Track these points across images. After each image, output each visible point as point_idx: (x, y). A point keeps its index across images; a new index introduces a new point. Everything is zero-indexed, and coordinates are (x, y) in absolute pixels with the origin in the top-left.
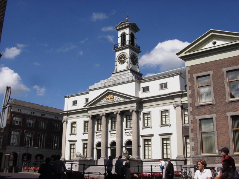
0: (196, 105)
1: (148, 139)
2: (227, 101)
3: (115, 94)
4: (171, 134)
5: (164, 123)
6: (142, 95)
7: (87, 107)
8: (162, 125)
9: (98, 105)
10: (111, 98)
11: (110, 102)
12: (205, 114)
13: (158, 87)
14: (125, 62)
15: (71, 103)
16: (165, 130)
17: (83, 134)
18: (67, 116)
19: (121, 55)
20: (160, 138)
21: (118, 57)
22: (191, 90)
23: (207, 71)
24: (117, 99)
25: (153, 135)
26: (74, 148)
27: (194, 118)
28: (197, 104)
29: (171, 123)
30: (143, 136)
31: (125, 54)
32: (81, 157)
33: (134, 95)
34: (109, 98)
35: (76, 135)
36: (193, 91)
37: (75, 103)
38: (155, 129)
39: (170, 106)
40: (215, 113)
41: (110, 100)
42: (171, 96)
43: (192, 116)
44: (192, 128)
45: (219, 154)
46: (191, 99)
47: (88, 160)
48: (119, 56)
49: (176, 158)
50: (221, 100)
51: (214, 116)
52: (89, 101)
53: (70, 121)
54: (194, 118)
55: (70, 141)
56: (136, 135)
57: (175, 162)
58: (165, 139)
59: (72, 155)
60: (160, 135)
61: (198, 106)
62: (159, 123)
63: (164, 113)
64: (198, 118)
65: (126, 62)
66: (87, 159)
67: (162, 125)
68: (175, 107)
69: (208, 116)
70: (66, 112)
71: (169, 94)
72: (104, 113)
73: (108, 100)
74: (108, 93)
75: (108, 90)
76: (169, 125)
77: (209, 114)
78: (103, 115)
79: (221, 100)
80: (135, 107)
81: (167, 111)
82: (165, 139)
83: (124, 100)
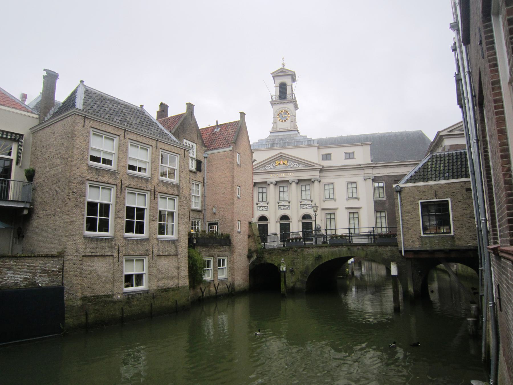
1: (331, 214)
4: (360, 208)
6: (326, 164)
8: (348, 199)
9: (262, 170)
10: (284, 164)
11: (282, 167)
16: (353, 204)
20: (346, 213)
24: (292, 166)
29: (359, 196)
33: (317, 162)
34: (282, 164)
39: (358, 177)
41: (282, 165)
42: (361, 167)
58: (354, 213)
62: (346, 197)
68: (365, 180)
71: (360, 165)
72: (274, 180)
75: (281, 153)
76: (357, 198)
78: (272, 183)
82: (354, 213)
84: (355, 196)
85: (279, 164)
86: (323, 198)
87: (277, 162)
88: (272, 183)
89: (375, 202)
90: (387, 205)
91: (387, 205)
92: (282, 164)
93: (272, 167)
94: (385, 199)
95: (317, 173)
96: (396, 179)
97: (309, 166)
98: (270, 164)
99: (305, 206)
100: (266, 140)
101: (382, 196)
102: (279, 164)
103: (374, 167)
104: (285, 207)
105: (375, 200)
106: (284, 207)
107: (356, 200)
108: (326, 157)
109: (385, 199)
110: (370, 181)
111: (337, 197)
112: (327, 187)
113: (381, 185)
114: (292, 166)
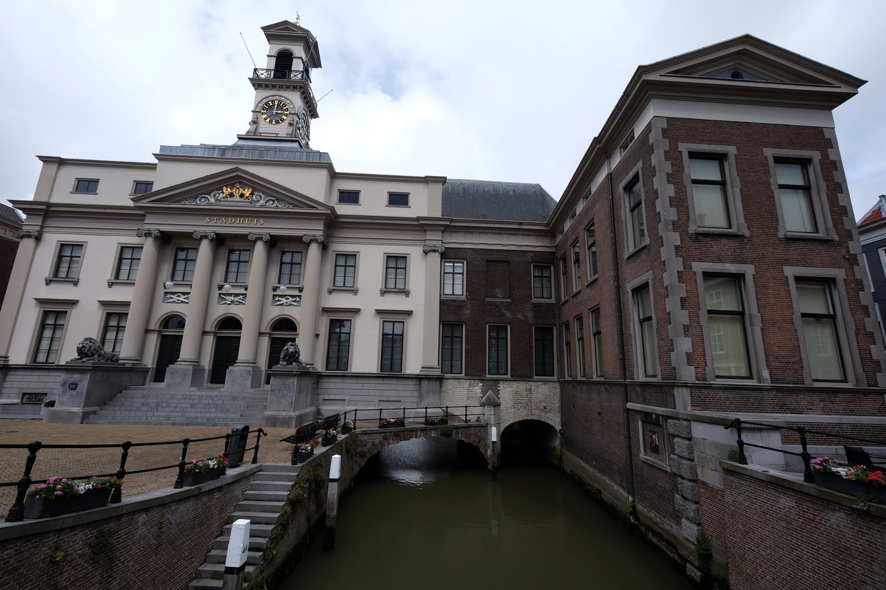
0: (692, 229)
3: (260, 186)
4: (409, 313)
5: (391, 285)
7: (144, 203)
9: (188, 204)
10: (242, 196)
11: (236, 203)
12: (720, 260)
13: (385, 199)
14: (282, 120)
15: (71, 184)
17: (111, 285)
18: (44, 221)
19: (273, 101)
21: (263, 103)
23: (721, 143)
24: (262, 202)
25: (360, 310)
26: (56, 327)
27: (687, 266)
30: (326, 311)
32: (99, 355)
33: (322, 200)
34: (237, 195)
35: (76, 283)
37: (87, 186)
38: (368, 296)
40: (752, 263)
42: (419, 226)
43: (681, 259)
44: (684, 295)
47: (127, 366)
49: (417, 372)
52: (155, 188)
53: (52, 241)
54: (687, 266)
55: (40, 301)
57: (415, 382)
59: (45, 345)
60: (379, 312)
62: (379, 284)
63: (396, 264)
64: (698, 267)
65: (286, 123)
66: (124, 364)
67: (383, 293)
68: (426, 253)
69: (731, 268)
70: (44, 207)
71: (418, 219)
73: (229, 199)
74: (235, 179)
75: (237, 169)
76: (407, 293)
77: (732, 262)
78: (205, 237)
80: (321, 233)
81: (404, 258)
83: (288, 208)
84: (400, 285)
85: (231, 195)
86: (328, 284)
87: (227, 190)
88: (205, 237)
89: (444, 303)
90: (467, 312)
91: (467, 312)
92: (237, 195)
93: (212, 200)
94: (464, 298)
95: (320, 226)
96: (490, 258)
97: (298, 206)
98: (209, 194)
99: (284, 300)
100: (224, 149)
101: (458, 291)
102: (231, 195)
103: (446, 226)
104: (236, 299)
105: (443, 297)
106: (232, 298)
107: (402, 297)
108: (350, 197)
109: (464, 298)
110: (436, 257)
111: (361, 284)
112: (341, 262)
113: (460, 267)
114: (262, 202)
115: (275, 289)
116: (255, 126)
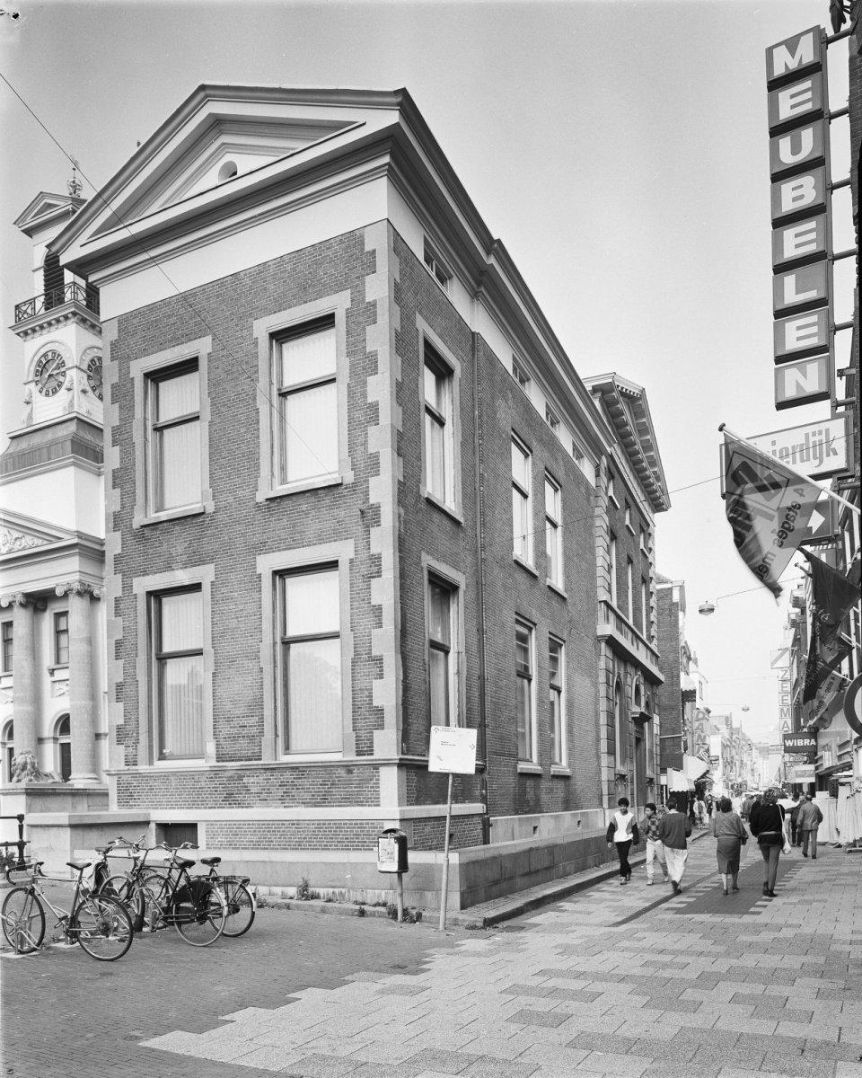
0: (139, 520)
2: (261, 497)
19: (45, 355)
21: (34, 363)
22: (121, 445)
27: (127, 587)
28: (142, 516)
31: (60, 349)
36: (127, 454)
43: (119, 576)
45: (219, 759)
46: (118, 491)
48: (36, 359)
50: (240, 493)
51: (205, 574)
54: (127, 587)
56: (83, 690)
61: (142, 527)
65: (63, 391)
77: (185, 566)
79: (240, 493)
115: (52, 672)
116: (30, 406)
